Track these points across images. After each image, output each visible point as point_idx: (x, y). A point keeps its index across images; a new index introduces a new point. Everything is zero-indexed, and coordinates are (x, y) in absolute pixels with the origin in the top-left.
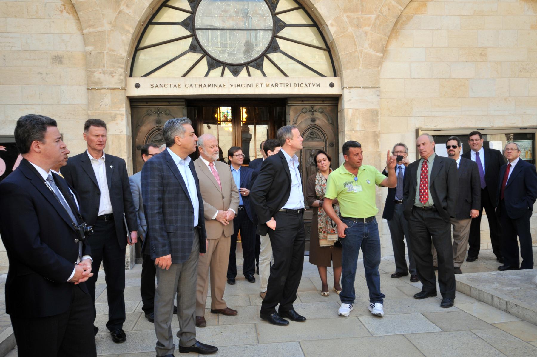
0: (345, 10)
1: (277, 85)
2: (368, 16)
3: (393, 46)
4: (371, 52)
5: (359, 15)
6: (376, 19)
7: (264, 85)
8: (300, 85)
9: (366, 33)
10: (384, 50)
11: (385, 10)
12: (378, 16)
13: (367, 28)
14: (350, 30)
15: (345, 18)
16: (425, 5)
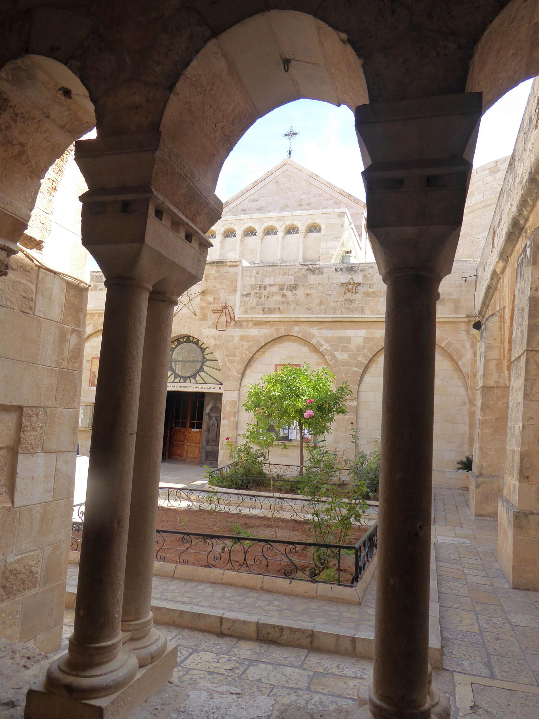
0: (226, 356)
1: (197, 387)
2: (236, 358)
3: (248, 372)
4: (236, 374)
5: (232, 358)
6: (240, 360)
7: (192, 387)
8: (206, 388)
9: (234, 366)
10: (243, 374)
11: (244, 356)
12: (241, 358)
13: (235, 364)
14: (228, 364)
15: (226, 359)
16: (265, 353)
